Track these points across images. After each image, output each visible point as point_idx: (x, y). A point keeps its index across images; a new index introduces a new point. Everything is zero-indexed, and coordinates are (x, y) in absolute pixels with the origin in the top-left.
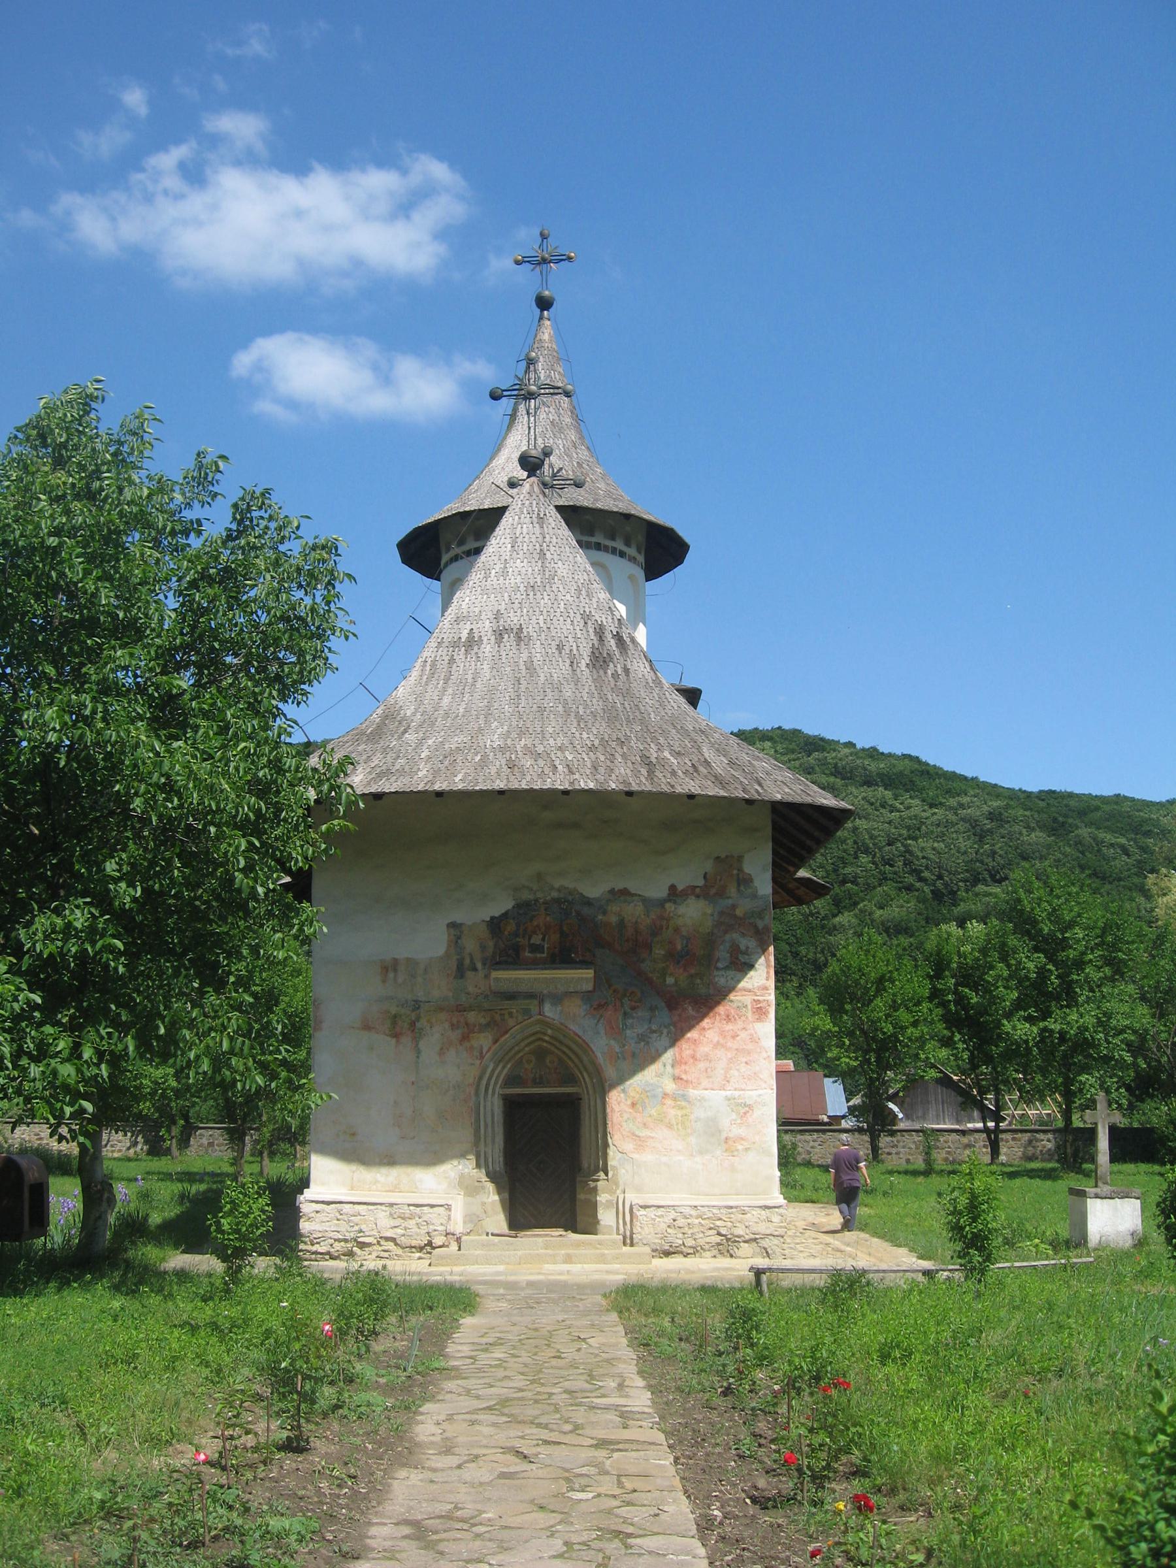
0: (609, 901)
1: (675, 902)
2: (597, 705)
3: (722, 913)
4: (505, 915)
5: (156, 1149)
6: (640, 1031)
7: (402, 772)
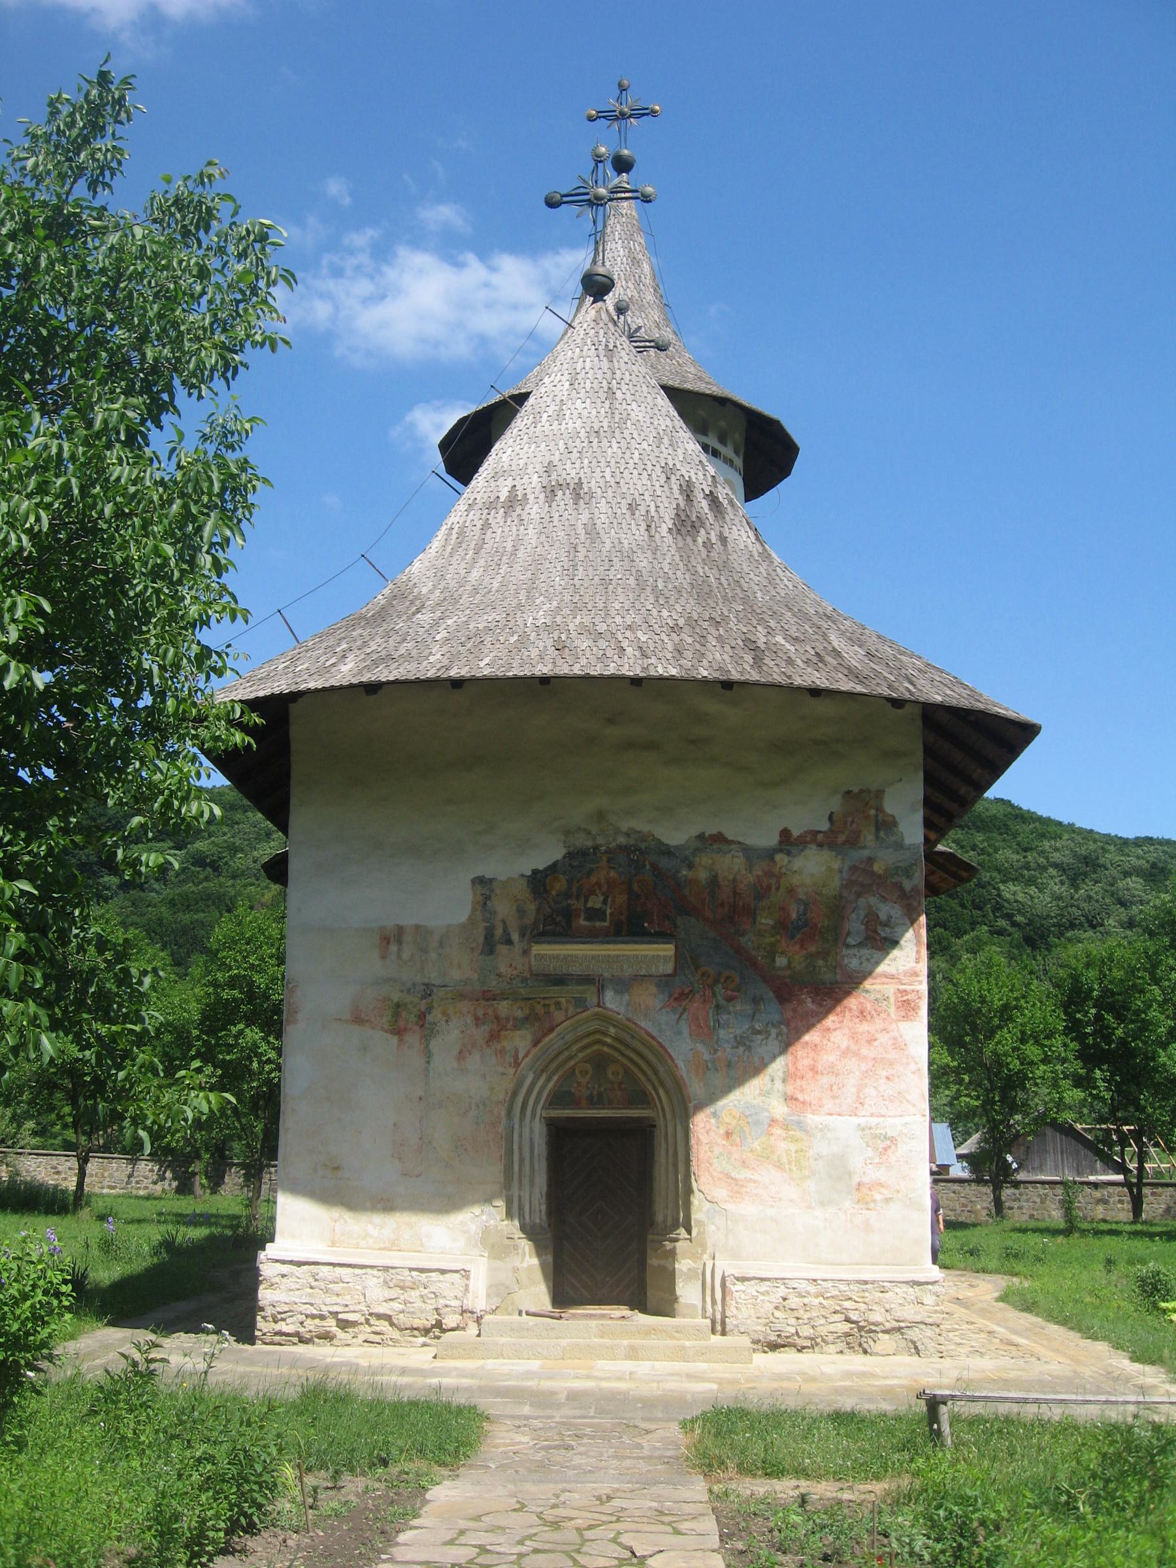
0: (696, 851)
1: (789, 853)
2: (683, 578)
3: (854, 869)
4: (553, 868)
5: (185, 1188)
6: (738, 1032)
7: (408, 657)
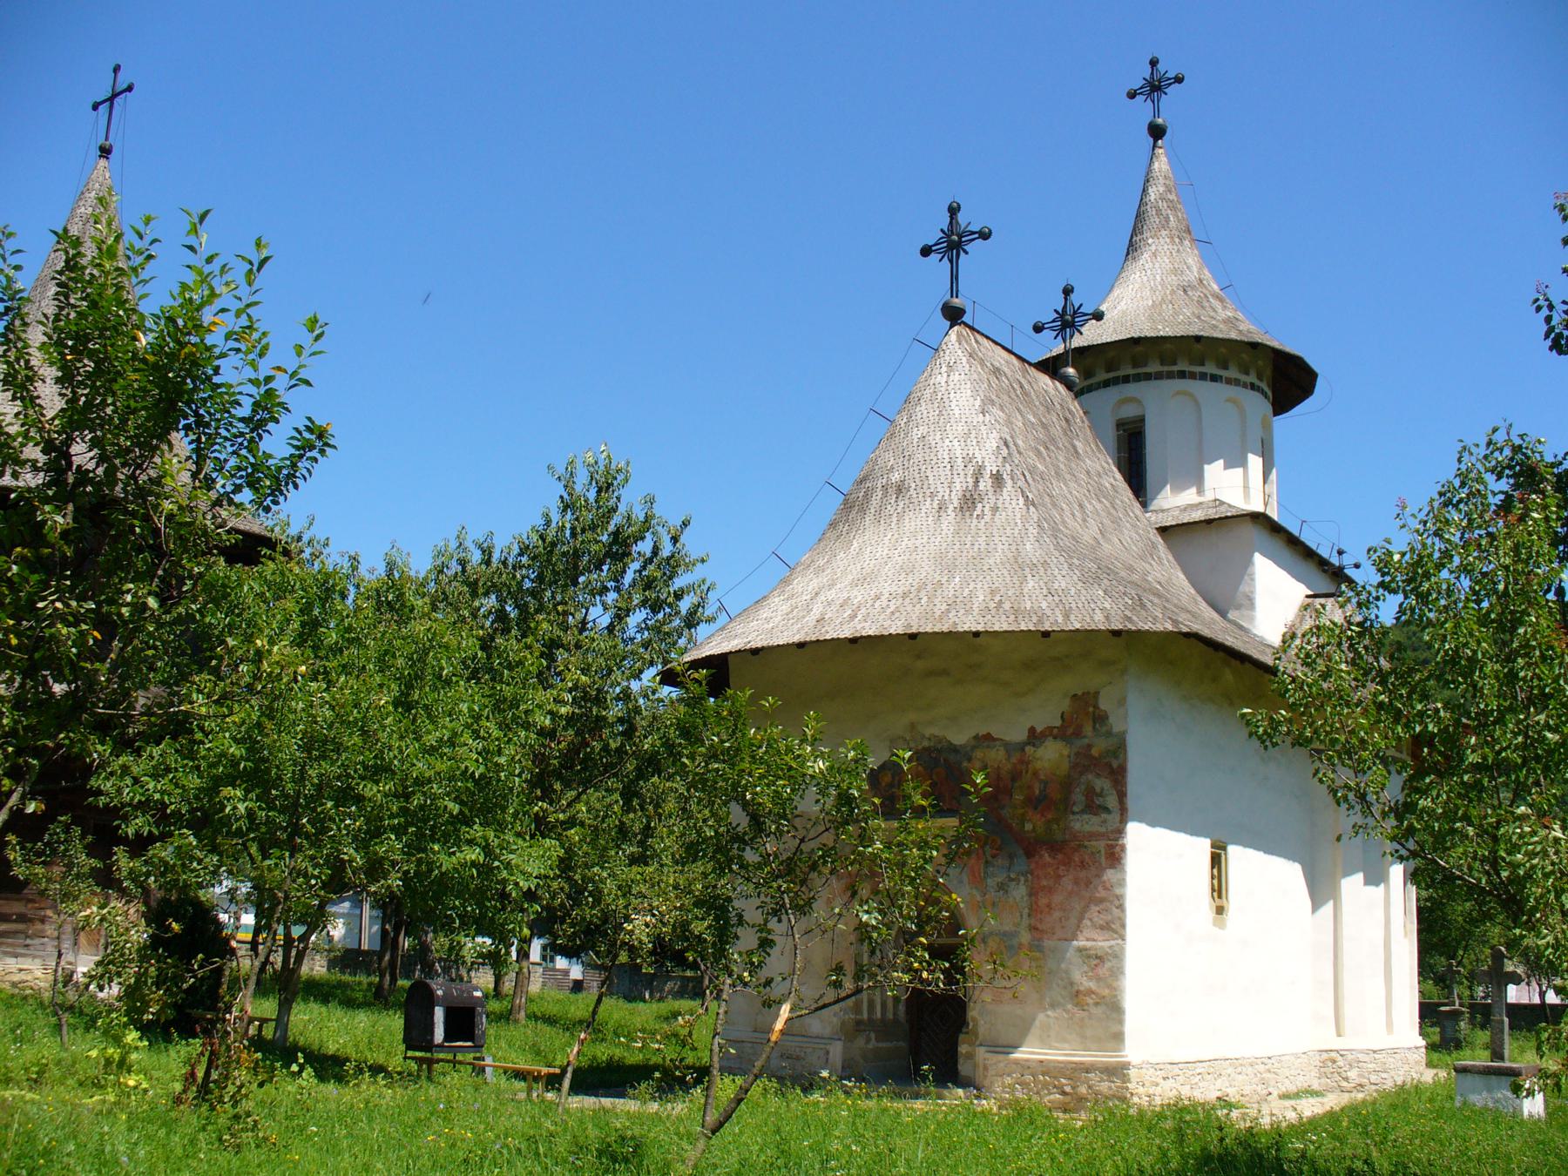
3: (1077, 754)
